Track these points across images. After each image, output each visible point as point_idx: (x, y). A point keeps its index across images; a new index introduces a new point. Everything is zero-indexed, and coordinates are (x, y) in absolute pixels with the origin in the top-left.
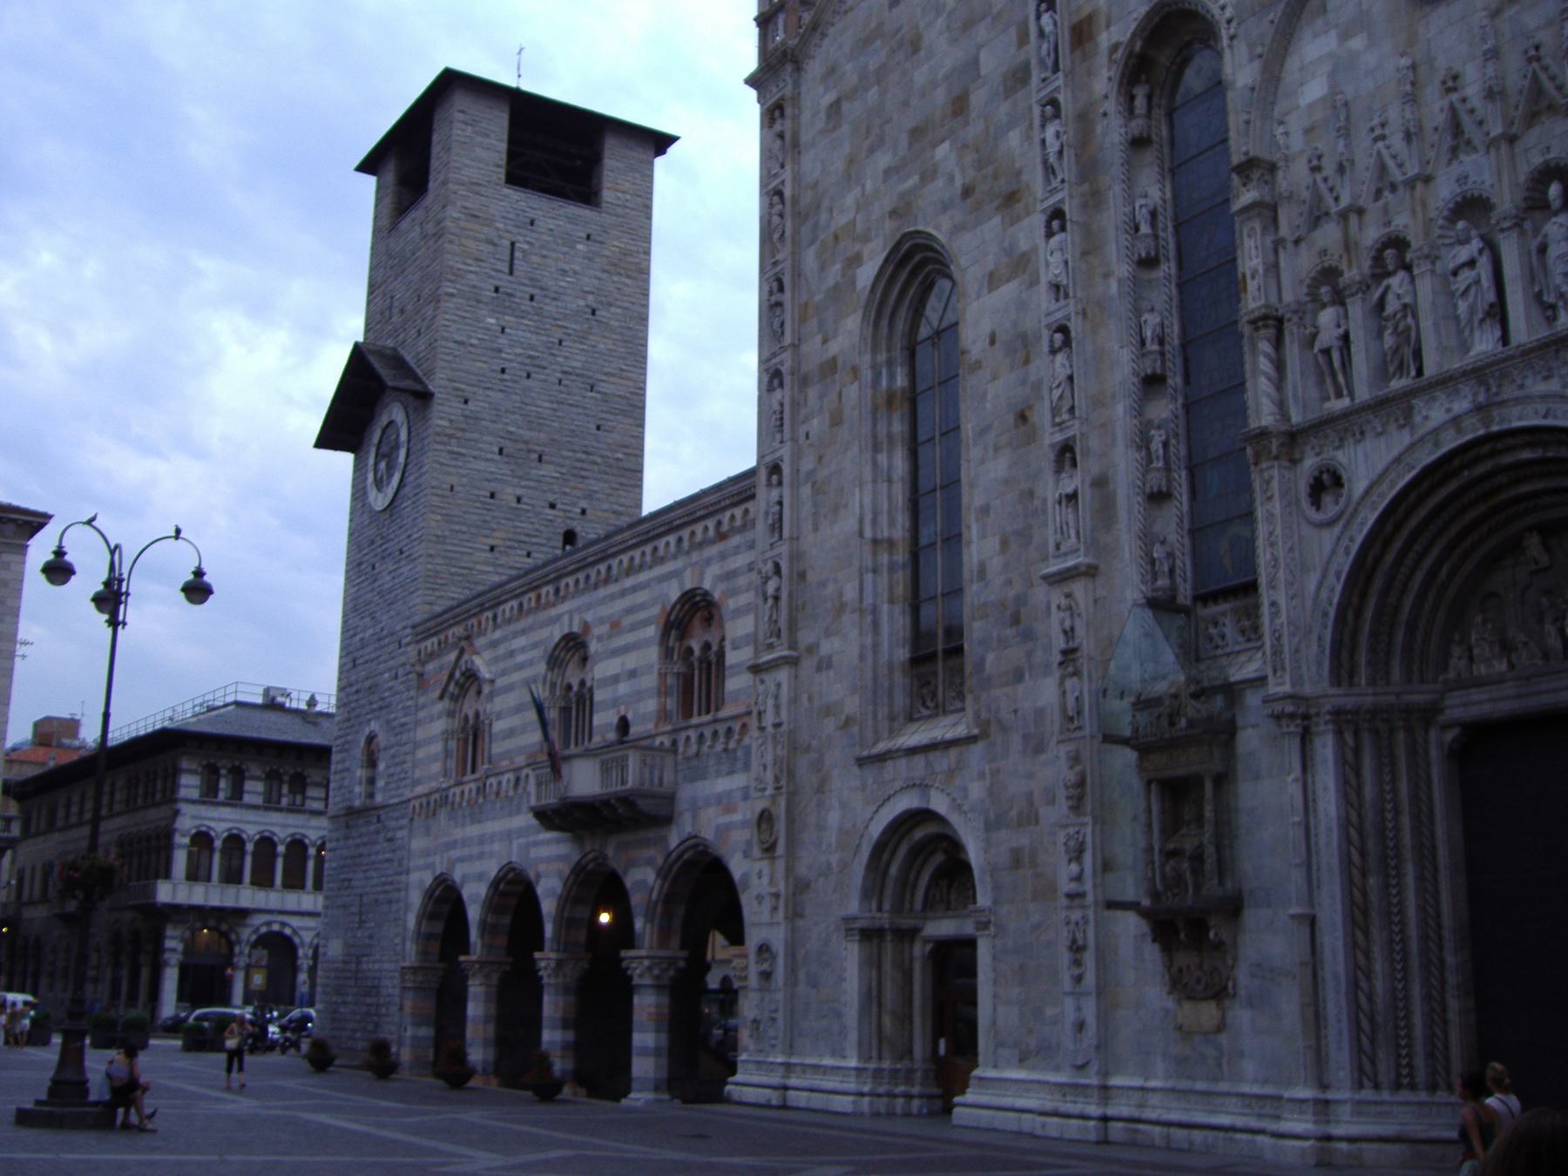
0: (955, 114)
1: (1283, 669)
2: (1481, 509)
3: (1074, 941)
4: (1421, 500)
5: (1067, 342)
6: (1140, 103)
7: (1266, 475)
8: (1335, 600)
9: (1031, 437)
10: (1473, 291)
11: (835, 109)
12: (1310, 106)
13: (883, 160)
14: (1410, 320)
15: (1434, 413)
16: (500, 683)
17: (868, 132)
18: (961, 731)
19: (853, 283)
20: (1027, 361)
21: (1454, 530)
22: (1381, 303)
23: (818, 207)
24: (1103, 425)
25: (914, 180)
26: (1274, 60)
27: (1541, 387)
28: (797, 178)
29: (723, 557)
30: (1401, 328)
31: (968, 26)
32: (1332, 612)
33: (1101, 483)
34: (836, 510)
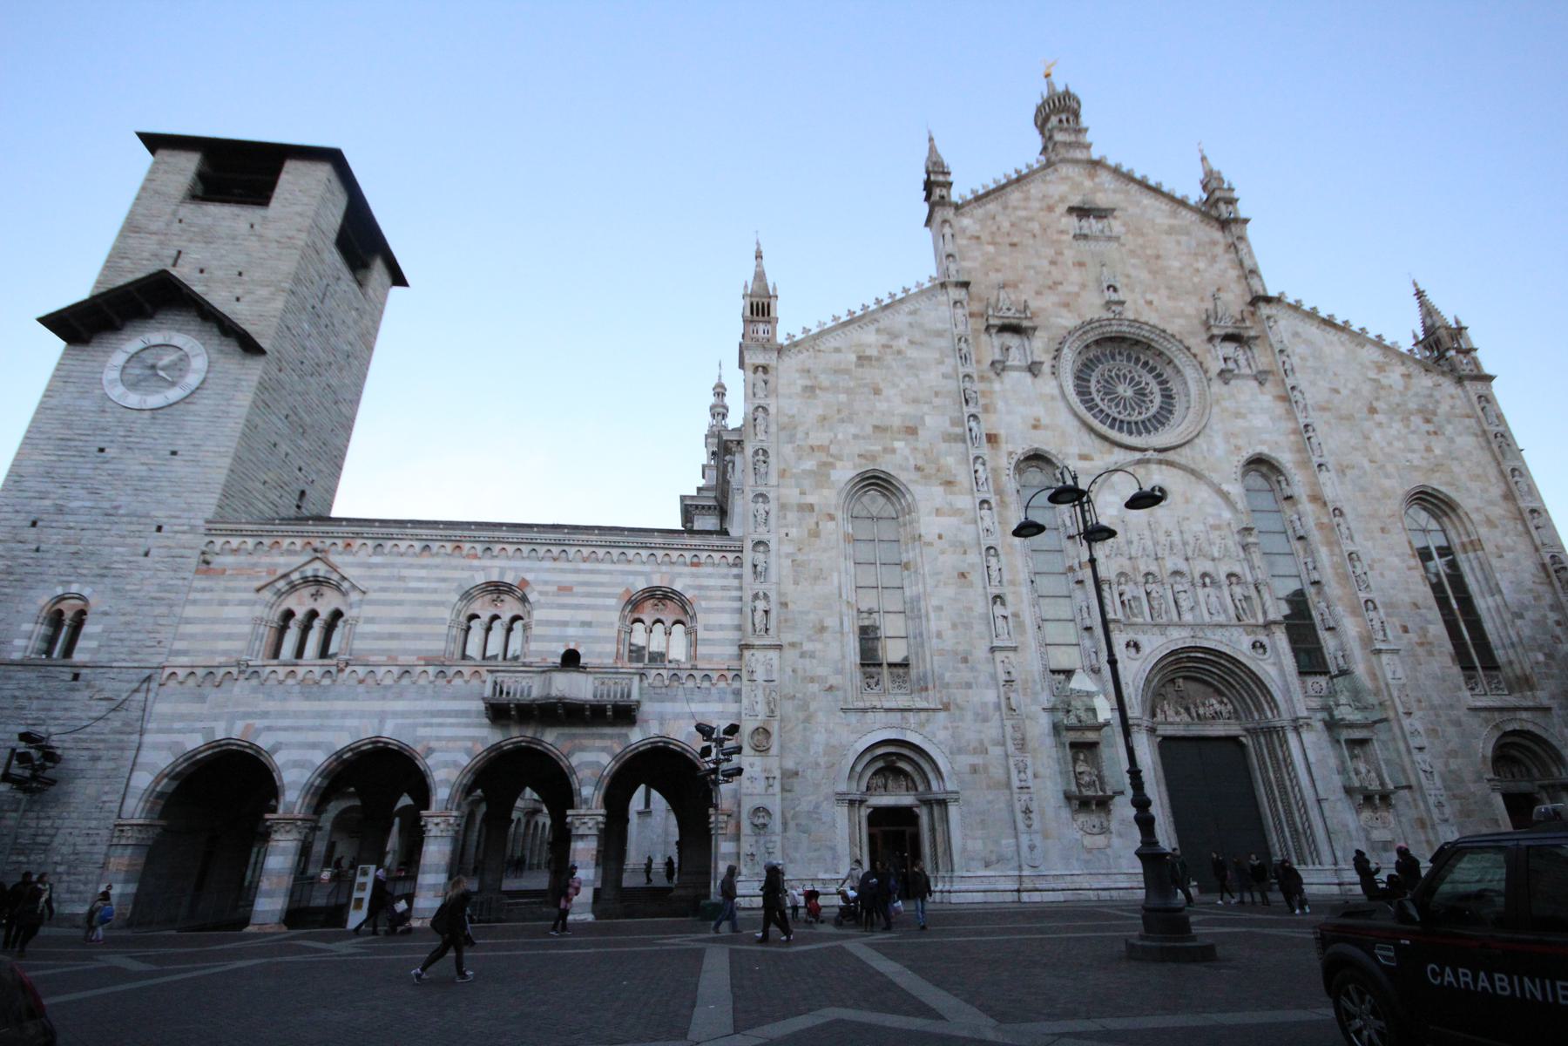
3: (1027, 808)
5: (996, 555)
9: (971, 585)
11: (810, 390)
12: (1111, 516)
13: (853, 430)
15: (1175, 633)
16: (372, 596)
17: (839, 411)
18: (924, 705)
19: (828, 476)
20: (965, 553)
23: (795, 428)
25: (878, 448)
29: (694, 575)
31: (916, 401)
33: (1016, 615)
34: (816, 578)
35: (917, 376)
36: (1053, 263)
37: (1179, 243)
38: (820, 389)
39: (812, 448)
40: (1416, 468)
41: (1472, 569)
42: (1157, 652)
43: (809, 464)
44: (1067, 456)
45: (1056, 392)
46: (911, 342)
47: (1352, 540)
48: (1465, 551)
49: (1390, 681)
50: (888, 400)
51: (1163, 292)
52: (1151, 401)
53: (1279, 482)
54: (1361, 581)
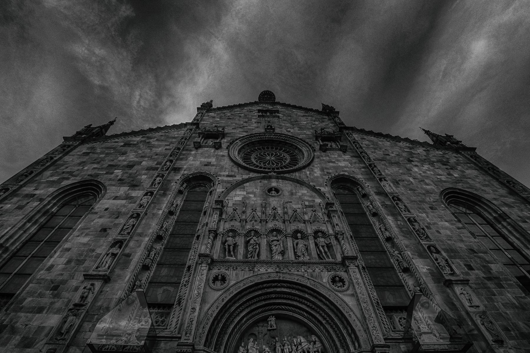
0: (127, 167)
1: (190, 334)
2: (264, 303)
4: (250, 293)
6: (185, 185)
7: (202, 268)
8: (214, 315)
10: (278, 246)
11: (86, 154)
14: (257, 246)
15: (263, 270)
17: (95, 160)
20: (117, 218)
21: (253, 307)
22: (249, 241)
24: (137, 241)
26: (229, 191)
27: (296, 273)
28: (60, 158)
30: (254, 248)
31: (142, 157)
32: (211, 320)
33: (128, 255)
35: (151, 149)
36: (246, 122)
37: (307, 118)
38: (93, 153)
39: (63, 172)
40: (445, 182)
41: (510, 232)
42: (242, 284)
43: (55, 178)
44: (220, 175)
45: (226, 154)
46: (157, 140)
47: (409, 211)
48: (500, 223)
49: (469, 309)
50: (128, 156)
51: (296, 129)
52: (285, 162)
53: (358, 189)
54: (422, 234)
